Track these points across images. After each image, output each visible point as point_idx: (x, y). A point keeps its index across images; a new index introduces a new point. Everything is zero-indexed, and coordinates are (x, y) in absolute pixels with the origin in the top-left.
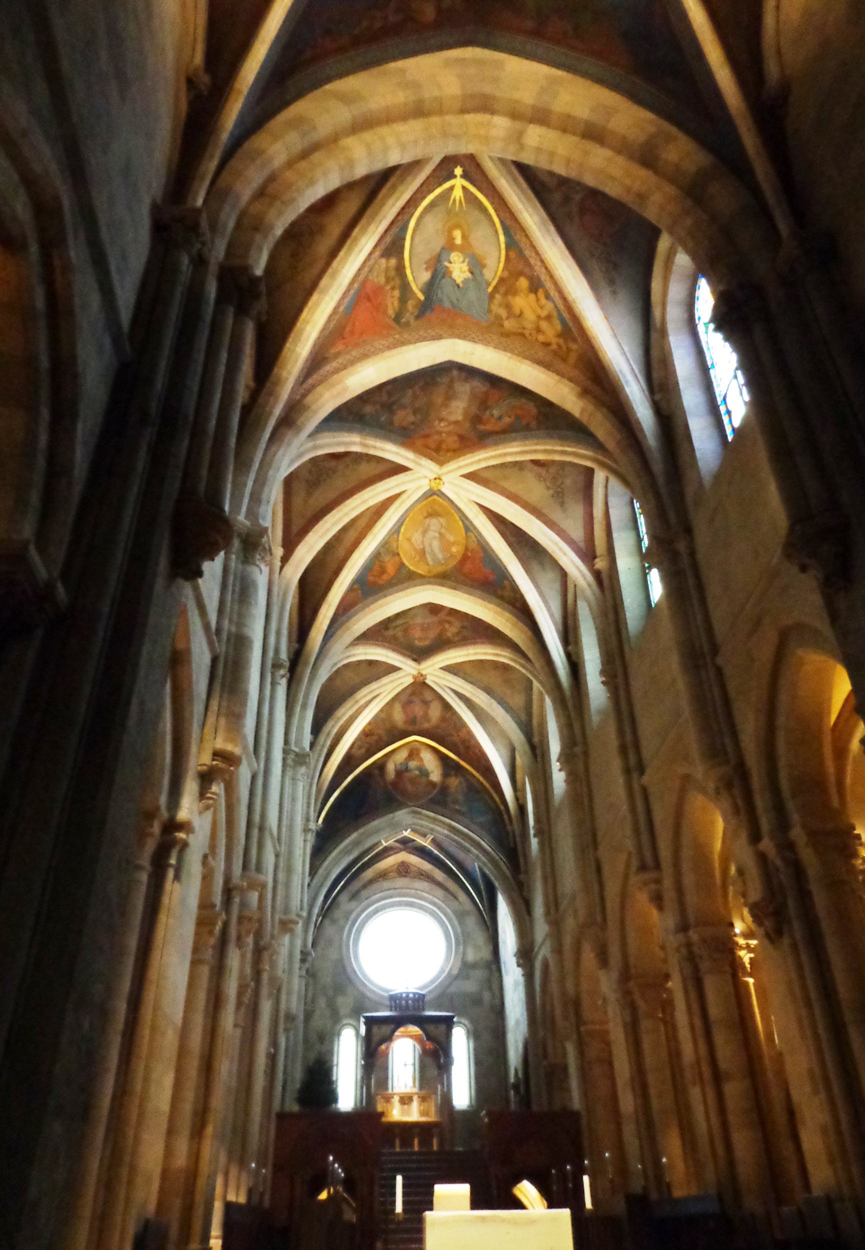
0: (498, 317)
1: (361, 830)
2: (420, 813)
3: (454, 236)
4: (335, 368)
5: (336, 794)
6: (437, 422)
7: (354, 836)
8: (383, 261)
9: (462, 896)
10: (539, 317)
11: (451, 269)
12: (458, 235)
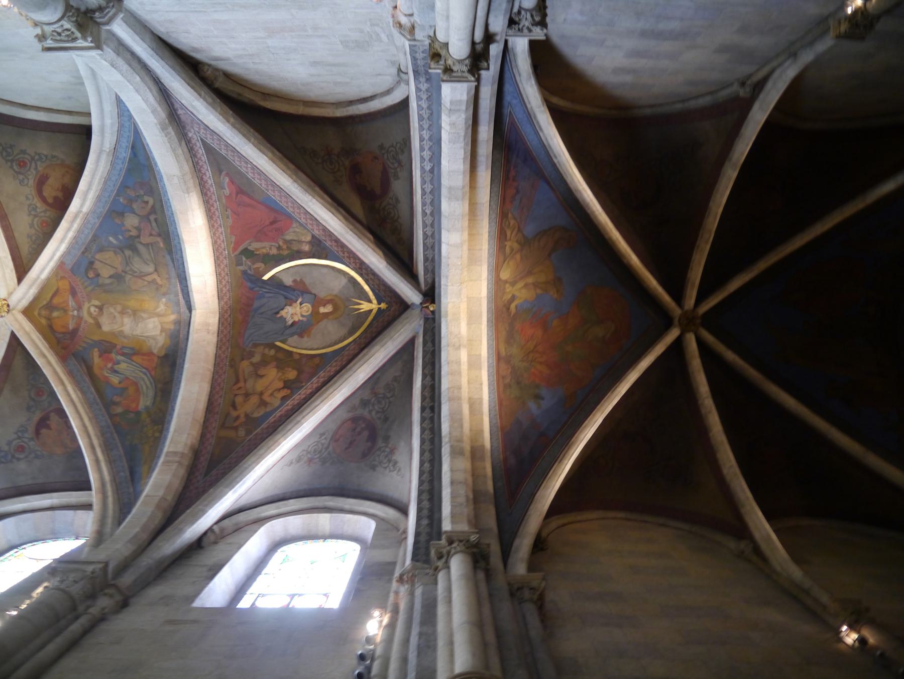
0: (251, 355)
3: (327, 305)
4: (206, 182)
6: (97, 303)
8: (309, 238)
10: (261, 394)
11: (294, 305)
12: (327, 309)
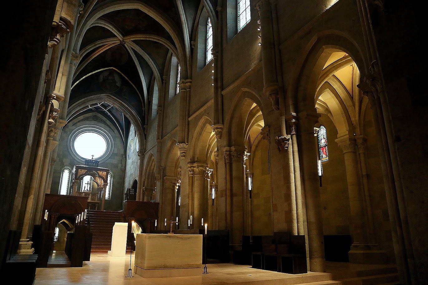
1: (86, 98)
2: (110, 97)
5: (77, 82)
7: (83, 100)
9: (116, 131)
